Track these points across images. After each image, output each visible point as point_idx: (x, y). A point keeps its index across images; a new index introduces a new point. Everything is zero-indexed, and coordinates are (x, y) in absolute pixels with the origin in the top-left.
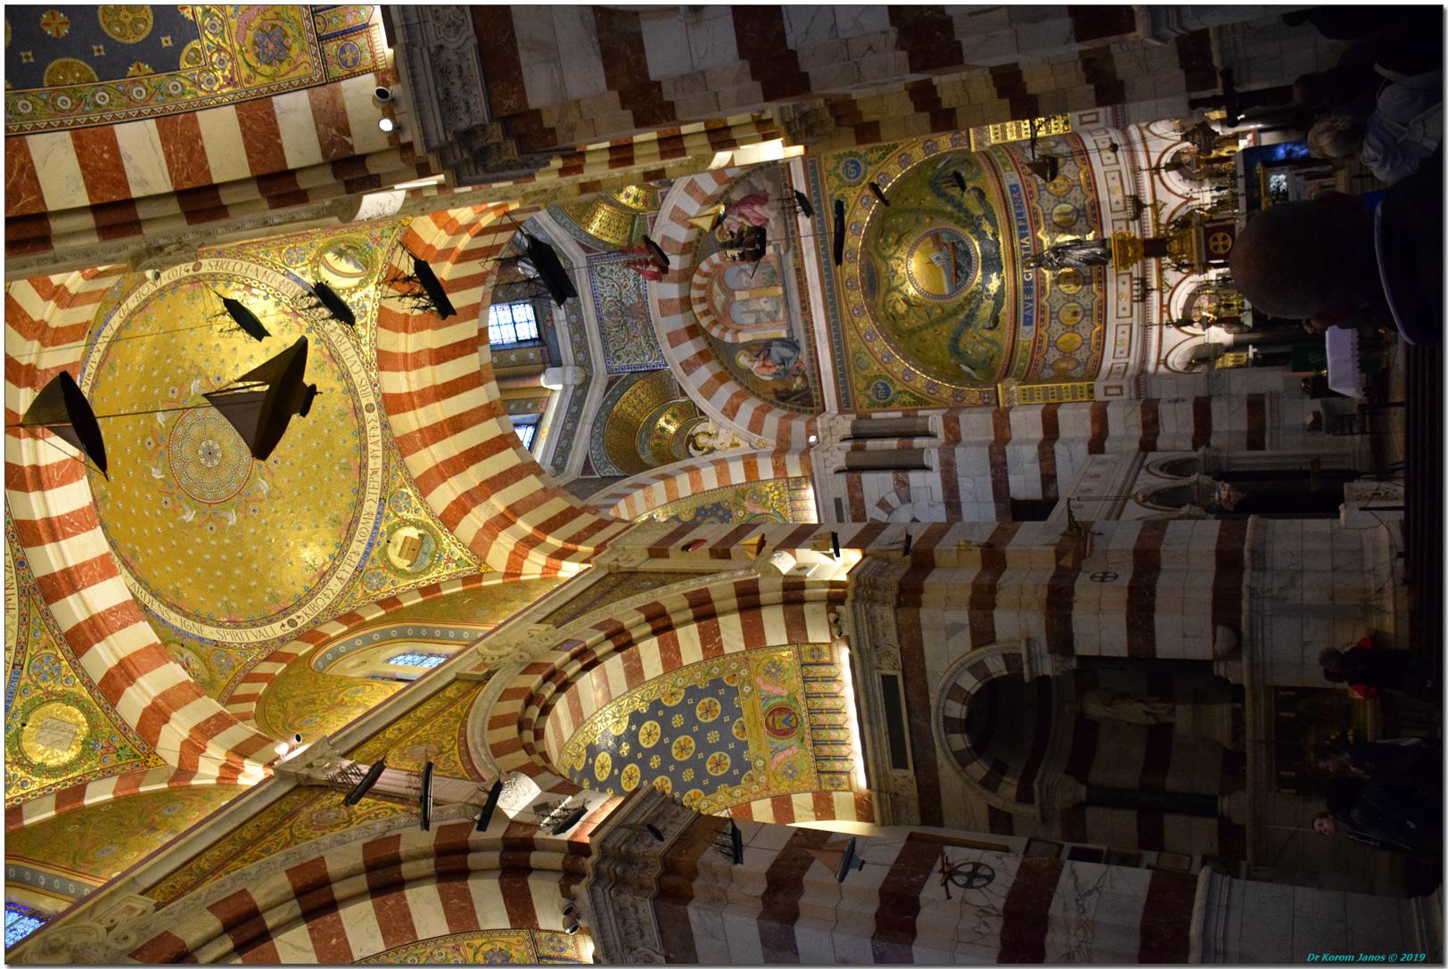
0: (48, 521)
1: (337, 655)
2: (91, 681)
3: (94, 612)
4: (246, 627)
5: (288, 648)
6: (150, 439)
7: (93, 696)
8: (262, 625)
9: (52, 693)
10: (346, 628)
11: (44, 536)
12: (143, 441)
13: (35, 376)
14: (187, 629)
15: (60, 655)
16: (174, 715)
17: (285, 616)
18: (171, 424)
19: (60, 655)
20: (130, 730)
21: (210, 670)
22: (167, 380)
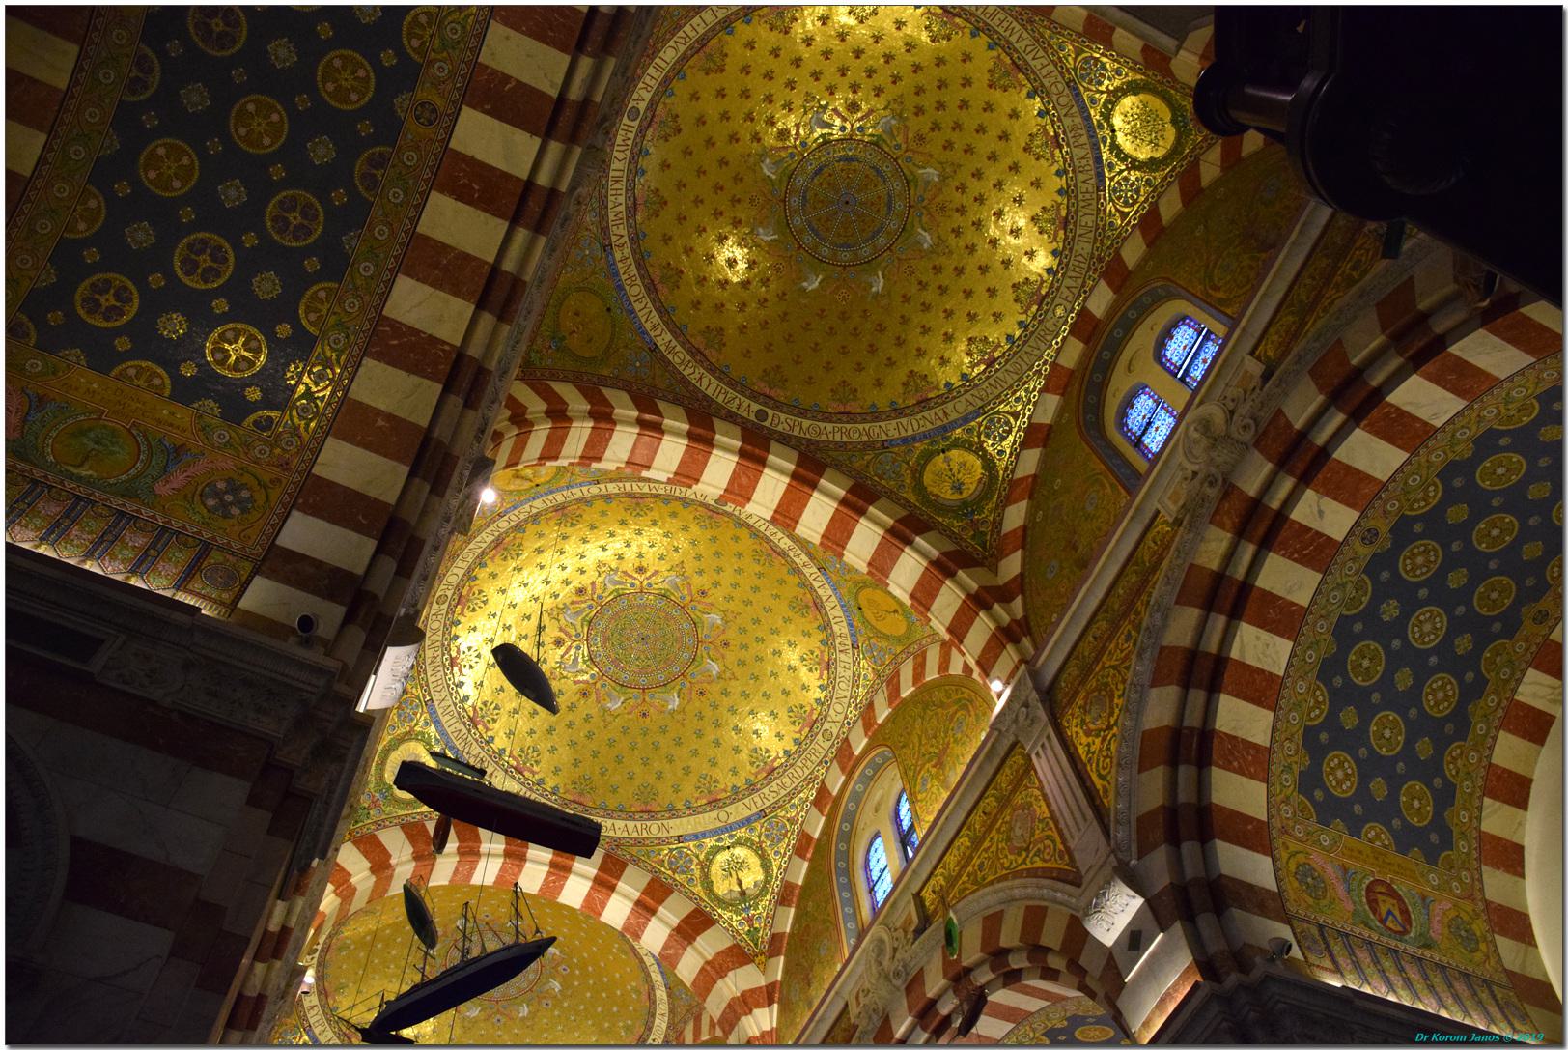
7: (418, 814)
13: (685, 939)
16: (373, 879)
20: (377, 829)
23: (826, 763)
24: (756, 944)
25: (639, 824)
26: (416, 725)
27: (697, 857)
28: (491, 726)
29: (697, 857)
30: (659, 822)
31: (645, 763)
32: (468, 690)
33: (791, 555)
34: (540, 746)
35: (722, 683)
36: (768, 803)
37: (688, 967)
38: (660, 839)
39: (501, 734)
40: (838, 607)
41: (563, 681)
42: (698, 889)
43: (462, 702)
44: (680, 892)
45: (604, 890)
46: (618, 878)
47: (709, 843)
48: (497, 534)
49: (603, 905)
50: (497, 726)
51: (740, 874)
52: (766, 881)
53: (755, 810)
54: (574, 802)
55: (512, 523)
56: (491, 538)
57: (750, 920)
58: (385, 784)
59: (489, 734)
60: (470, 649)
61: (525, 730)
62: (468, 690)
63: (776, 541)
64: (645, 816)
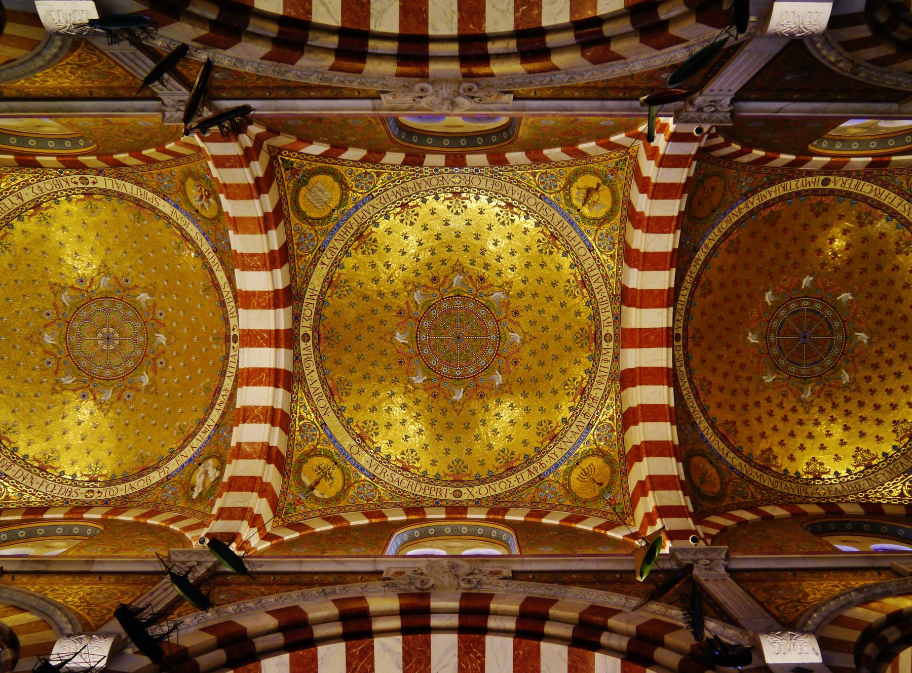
0: (277, 346)
1: (60, 140)
2: (285, 223)
3: (269, 273)
4: (129, 196)
5: (101, 164)
6: (160, 366)
8: (113, 192)
9: (310, 224)
10: (38, 158)
11: (282, 336)
12: (167, 366)
14: (185, 219)
15: (295, 247)
17: (90, 188)
18: (138, 371)
19: (295, 247)
21: (183, 183)
22: (132, 407)
23: (437, 503)
24: (286, 513)
25: (321, 390)
26: (354, 191)
27: (318, 443)
28: (359, 251)
29: (318, 443)
30: (328, 405)
31: (366, 377)
32: (384, 224)
33: (588, 402)
34: (352, 295)
35: (449, 407)
36: (381, 477)
37: (238, 468)
38: (317, 410)
39: (355, 261)
40: (565, 452)
41: (406, 293)
42: (297, 455)
43: (374, 222)
44: (289, 441)
45: (272, 379)
46: (284, 388)
47: (332, 448)
48: (522, 200)
49: (259, 383)
50: (360, 256)
51: (323, 480)
52: (327, 501)
53: (371, 470)
54: (319, 335)
55: (534, 208)
56: (516, 197)
57: (298, 502)
58: (309, 178)
59: (353, 252)
60: (417, 215)
61: (363, 280)
62: (384, 224)
63: (594, 387)
64: (328, 393)
